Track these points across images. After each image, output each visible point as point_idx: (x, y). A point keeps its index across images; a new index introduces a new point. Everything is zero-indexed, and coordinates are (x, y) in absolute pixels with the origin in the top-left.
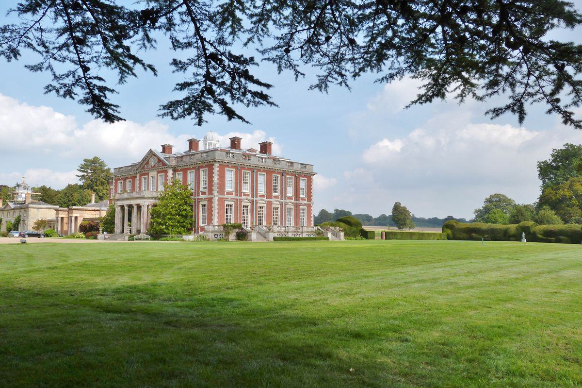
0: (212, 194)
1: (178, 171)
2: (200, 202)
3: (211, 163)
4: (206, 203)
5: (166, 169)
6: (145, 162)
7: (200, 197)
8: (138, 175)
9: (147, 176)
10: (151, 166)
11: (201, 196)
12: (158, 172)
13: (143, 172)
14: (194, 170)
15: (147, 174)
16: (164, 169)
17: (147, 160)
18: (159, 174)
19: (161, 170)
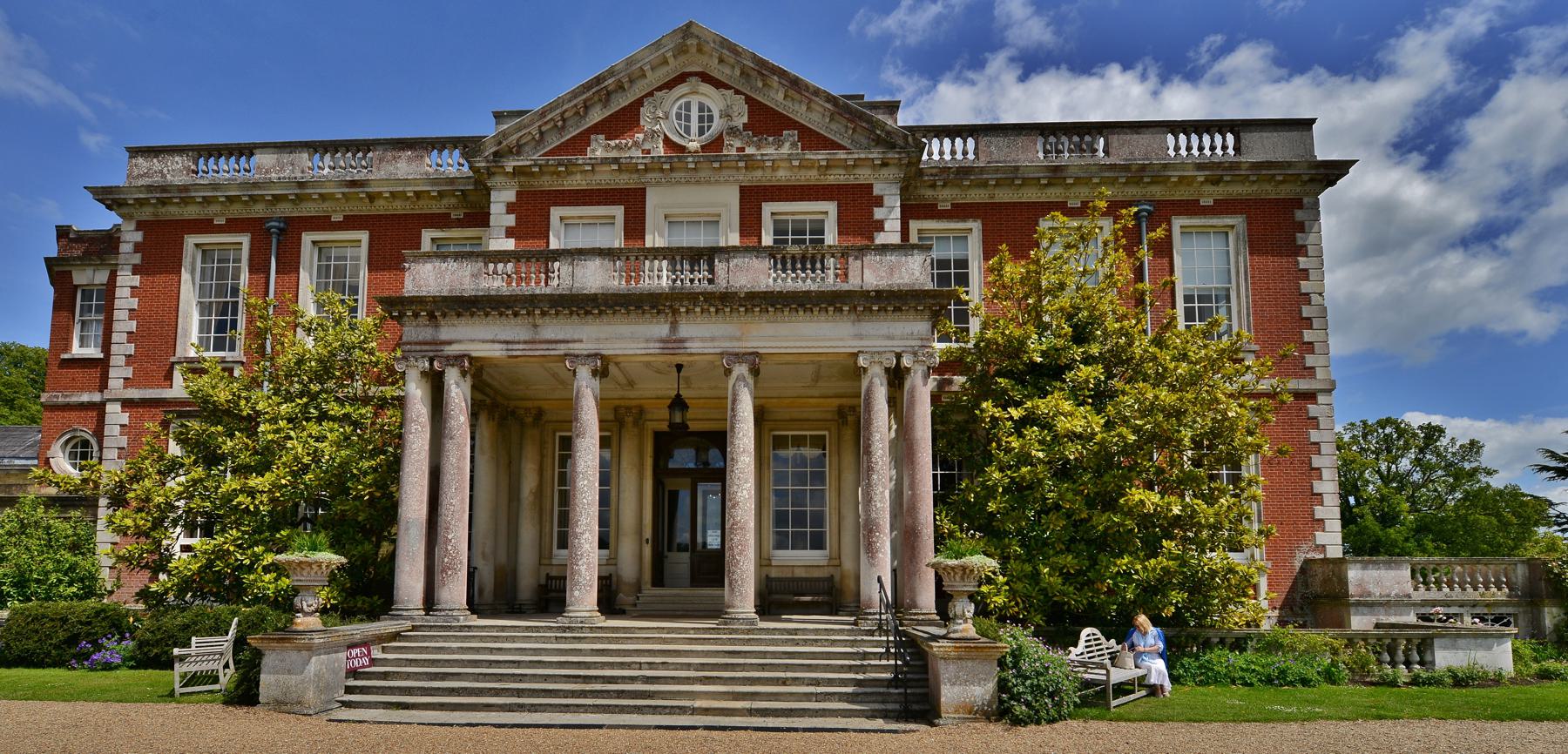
5: (863, 175)
6: (596, 116)
8: (502, 198)
16: (836, 177)
17: (622, 102)
19: (811, 177)
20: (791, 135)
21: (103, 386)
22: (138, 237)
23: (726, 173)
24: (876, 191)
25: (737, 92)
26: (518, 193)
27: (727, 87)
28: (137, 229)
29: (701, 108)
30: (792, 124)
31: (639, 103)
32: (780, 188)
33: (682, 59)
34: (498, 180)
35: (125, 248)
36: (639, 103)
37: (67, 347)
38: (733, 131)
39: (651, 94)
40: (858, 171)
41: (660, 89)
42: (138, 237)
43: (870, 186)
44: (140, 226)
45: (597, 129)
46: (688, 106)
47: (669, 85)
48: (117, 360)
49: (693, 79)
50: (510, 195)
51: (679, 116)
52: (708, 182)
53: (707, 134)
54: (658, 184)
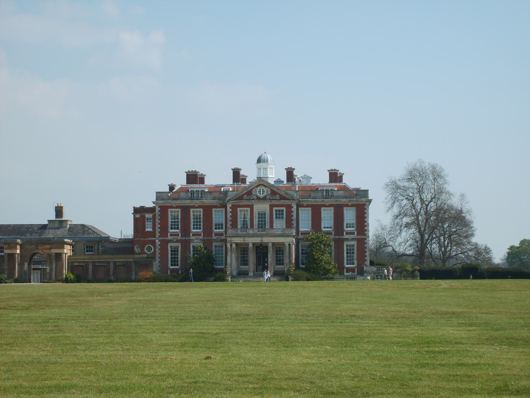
0: (366, 235)
1: (302, 206)
2: (345, 242)
3: (363, 203)
4: (355, 243)
5: (290, 203)
6: (245, 192)
7: (344, 237)
9: (249, 209)
10: (258, 198)
11: (346, 236)
12: (271, 207)
13: (242, 204)
14: (332, 208)
15: (251, 207)
18: (274, 209)
20: (278, 196)
21: (155, 237)
22: (159, 209)
23: (267, 203)
24: (292, 206)
25: (269, 188)
26: (232, 205)
27: (267, 187)
28: (159, 207)
29: (263, 190)
30: (278, 194)
31: (252, 189)
32: (276, 205)
33: (260, 182)
34: (228, 203)
35: (157, 211)
36: (252, 189)
37: (145, 230)
38: (268, 195)
39: (254, 188)
40: (289, 203)
41: (255, 187)
42: (159, 209)
43: (291, 204)
44: (159, 207)
45: (245, 194)
46: (260, 189)
47: (257, 186)
48: (157, 232)
49: (262, 186)
50: (230, 206)
51: (259, 192)
52: (264, 204)
53: (264, 195)
54: (256, 204)
